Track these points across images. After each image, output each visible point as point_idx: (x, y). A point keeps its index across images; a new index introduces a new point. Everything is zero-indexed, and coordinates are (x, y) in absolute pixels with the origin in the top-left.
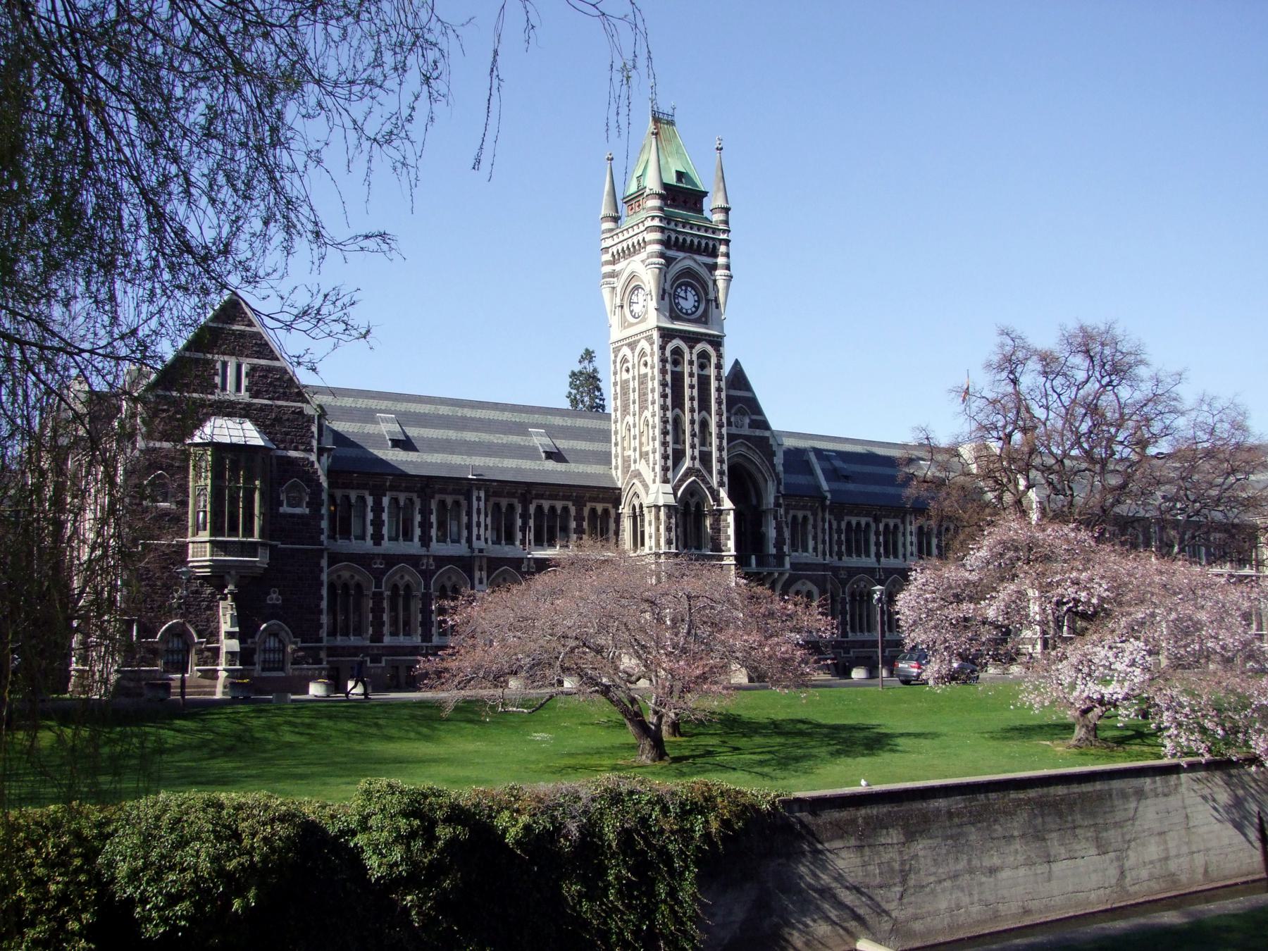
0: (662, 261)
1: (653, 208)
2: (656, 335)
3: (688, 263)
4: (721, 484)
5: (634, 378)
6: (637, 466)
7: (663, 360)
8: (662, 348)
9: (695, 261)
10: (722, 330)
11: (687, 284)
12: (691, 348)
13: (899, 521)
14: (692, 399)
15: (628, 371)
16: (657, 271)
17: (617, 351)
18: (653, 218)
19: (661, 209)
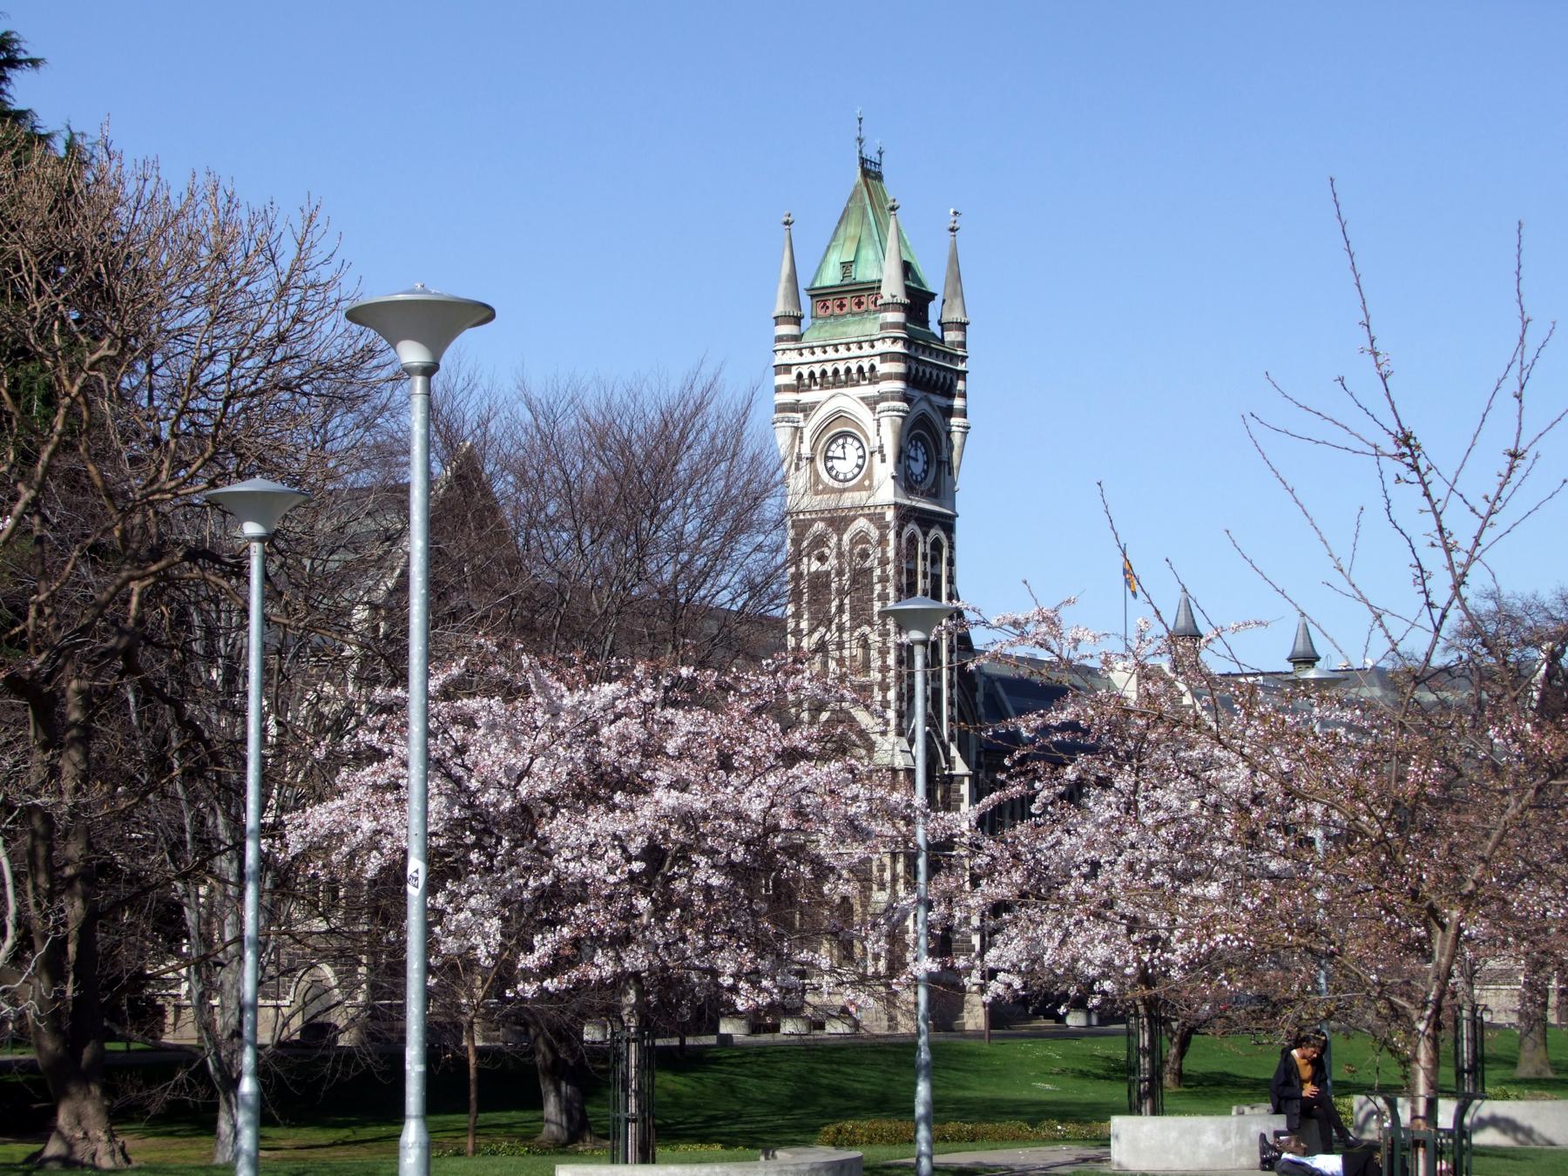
0: (904, 406)
1: (894, 325)
2: (890, 515)
3: (924, 406)
5: (840, 573)
8: (898, 535)
9: (930, 403)
10: (953, 509)
11: (919, 438)
12: (925, 534)
16: (899, 420)
18: (895, 340)
19: (904, 327)
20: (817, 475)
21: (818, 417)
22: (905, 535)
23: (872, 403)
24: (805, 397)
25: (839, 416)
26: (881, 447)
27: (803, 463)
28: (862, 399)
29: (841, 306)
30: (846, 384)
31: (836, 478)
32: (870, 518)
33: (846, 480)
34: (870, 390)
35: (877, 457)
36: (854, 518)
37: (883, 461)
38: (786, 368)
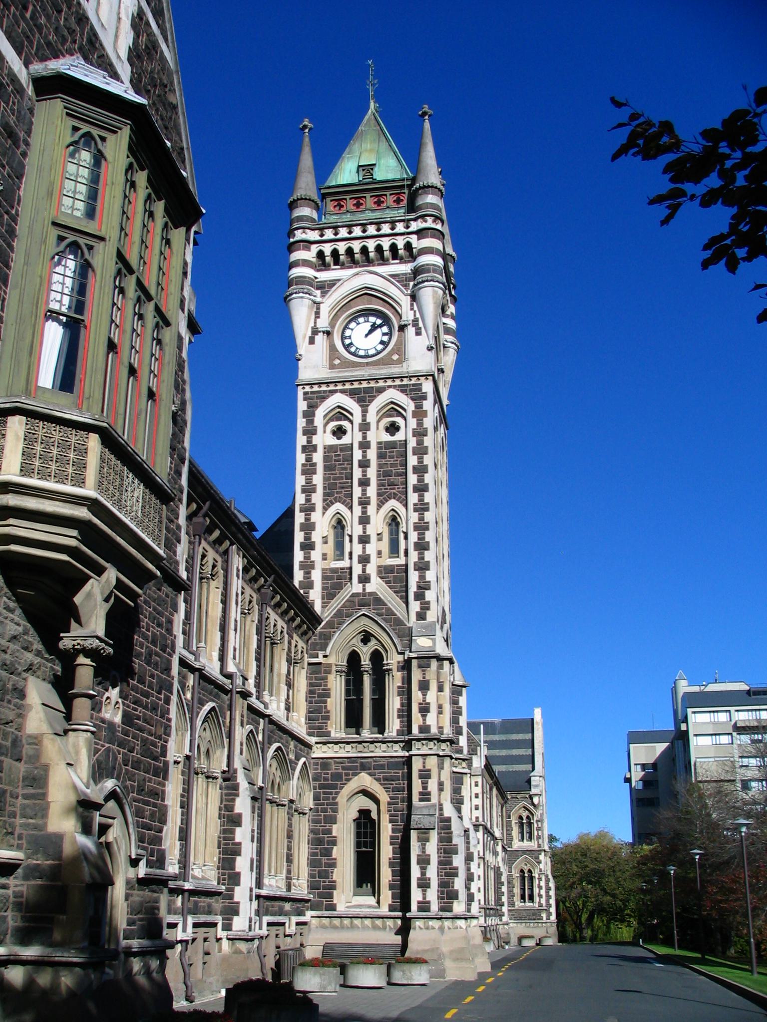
5: (365, 445)
6: (370, 588)
20: (332, 348)
24: (324, 276)
25: (367, 293)
27: (319, 338)
28: (393, 276)
32: (403, 389)
36: (381, 390)
37: (418, 333)
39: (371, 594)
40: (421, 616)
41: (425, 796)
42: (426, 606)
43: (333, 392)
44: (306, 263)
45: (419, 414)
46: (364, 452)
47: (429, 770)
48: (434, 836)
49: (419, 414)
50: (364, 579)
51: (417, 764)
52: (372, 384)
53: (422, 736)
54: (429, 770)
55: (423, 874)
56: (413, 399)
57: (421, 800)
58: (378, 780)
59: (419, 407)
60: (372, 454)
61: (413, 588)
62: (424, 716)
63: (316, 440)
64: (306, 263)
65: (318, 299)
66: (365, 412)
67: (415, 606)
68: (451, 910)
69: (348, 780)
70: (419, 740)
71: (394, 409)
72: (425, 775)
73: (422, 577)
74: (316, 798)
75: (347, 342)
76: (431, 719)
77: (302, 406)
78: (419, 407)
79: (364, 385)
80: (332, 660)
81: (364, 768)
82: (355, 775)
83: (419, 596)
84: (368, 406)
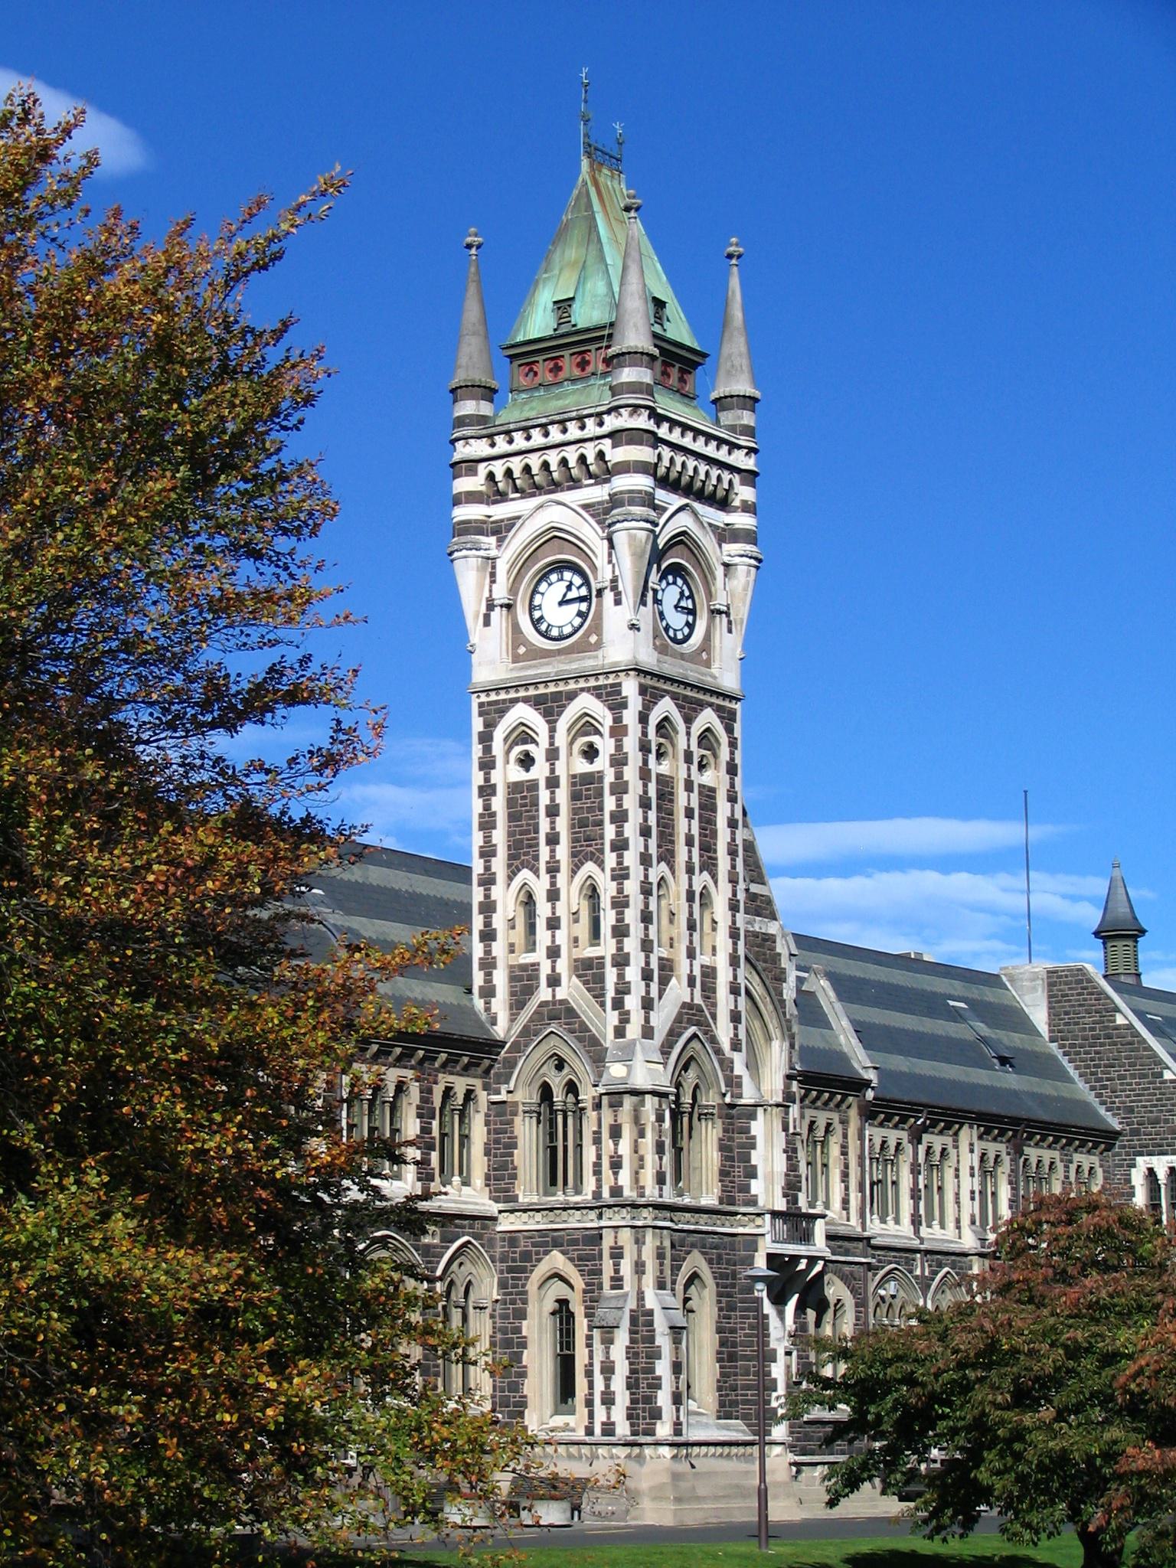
2: (630, 688)
3: (684, 521)
4: (736, 1046)
5: (553, 783)
6: (561, 993)
7: (644, 748)
8: (643, 719)
12: (688, 720)
13: (949, 1140)
14: (689, 842)
15: (527, 761)
17: (493, 713)
18: (636, 408)
20: (516, 628)
21: (518, 540)
22: (654, 719)
23: (601, 513)
24: (500, 511)
25: (554, 536)
26: (614, 580)
27: (497, 615)
28: (585, 507)
29: (556, 369)
30: (555, 486)
31: (545, 635)
32: (597, 692)
33: (561, 638)
34: (597, 493)
35: (609, 596)
36: (572, 696)
37: (618, 602)
38: (470, 465)
39: (563, 1002)
40: (620, 1032)
41: (617, 1282)
42: (625, 1018)
43: (515, 701)
44: (473, 497)
45: (619, 731)
46: (553, 793)
47: (621, 1248)
48: (622, 1338)
49: (619, 731)
50: (554, 981)
51: (608, 1241)
52: (562, 687)
53: (612, 1201)
54: (621, 1248)
55: (607, 1386)
56: (610, 709)
57: (613, 1288)
58: (571, 1260)
59: (618, 720)
60: (562, 796)
61: (610, 993)
62: (616, 1174)
63: (496, 777)
64: (473, 497)
65: (493, 553)
66: (552, 730)
67: (613, 1018)
68: (652, 1433)
69: (539, 1260)
70: (609, 1207)
71: (587, 726)
72: (617, 1254)
73: (621, 976)
74: (502, 1285)
75: (537, 614)
76: (625, 1178)
77: (478, 724)
78: (618, 720)
79: (552, 688)
80: (519, 1097)
81: (557, 1244)
82: (546, 1253)
83: (618, 1004)
84: (556, 721)
